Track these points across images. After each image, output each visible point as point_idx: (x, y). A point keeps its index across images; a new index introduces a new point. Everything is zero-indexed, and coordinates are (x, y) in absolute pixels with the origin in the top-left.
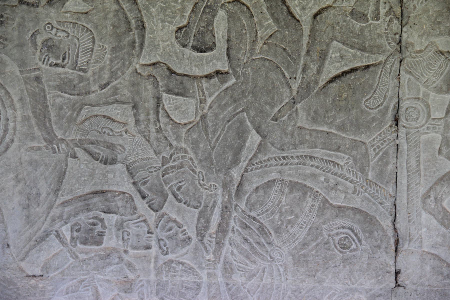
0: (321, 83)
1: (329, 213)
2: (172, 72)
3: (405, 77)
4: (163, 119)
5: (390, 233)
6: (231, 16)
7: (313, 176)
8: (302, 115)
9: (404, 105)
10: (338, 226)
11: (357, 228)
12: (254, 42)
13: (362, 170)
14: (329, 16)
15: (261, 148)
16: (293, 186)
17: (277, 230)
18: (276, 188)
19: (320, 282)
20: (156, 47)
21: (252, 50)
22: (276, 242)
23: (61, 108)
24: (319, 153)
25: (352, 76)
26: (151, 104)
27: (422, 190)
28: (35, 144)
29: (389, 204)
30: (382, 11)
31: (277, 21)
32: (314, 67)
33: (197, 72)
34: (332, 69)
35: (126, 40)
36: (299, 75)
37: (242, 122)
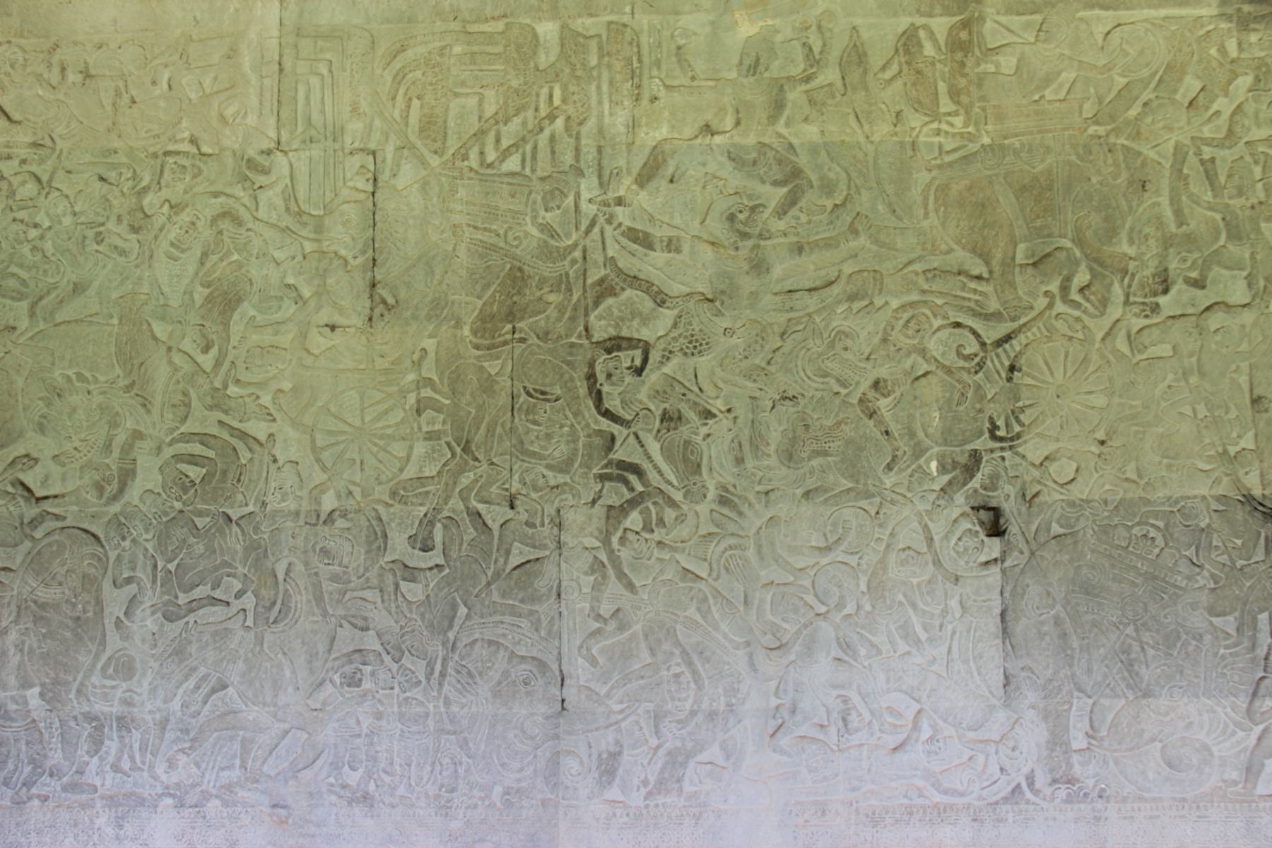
0: (508, 571)
1: (515, 661)
2: (406, 566)
3: (563, 565)
4: (400, 599)
5: (557, 673)
6: (445, 527)
7: (504, 635)
8: (495, 593)
9: (564, 584)
10: (522, 670)
11: (535, 670)
12: (461, 544)
13: (537, 630)
14: (511, 525)
15: (468, 617)
16: (490, 642)
17: (480, 674)
18: (479, 644)
19: (510, 709)
20: (394, 549)
21: (460, 550)
22: (480, 682)
23: (331, 594)
24: (508, 619)
25: (528, 566)
26: (392, 588)
27: (578, 642)
28: (315, 619)
29: (555, 653)
30: (546, 521)
31: (476, 529)
32: (502, 560)
33: (423, 566)
34: (515, 561)
35: (375, 546)
36: (492, 566)
37: (454, 599)
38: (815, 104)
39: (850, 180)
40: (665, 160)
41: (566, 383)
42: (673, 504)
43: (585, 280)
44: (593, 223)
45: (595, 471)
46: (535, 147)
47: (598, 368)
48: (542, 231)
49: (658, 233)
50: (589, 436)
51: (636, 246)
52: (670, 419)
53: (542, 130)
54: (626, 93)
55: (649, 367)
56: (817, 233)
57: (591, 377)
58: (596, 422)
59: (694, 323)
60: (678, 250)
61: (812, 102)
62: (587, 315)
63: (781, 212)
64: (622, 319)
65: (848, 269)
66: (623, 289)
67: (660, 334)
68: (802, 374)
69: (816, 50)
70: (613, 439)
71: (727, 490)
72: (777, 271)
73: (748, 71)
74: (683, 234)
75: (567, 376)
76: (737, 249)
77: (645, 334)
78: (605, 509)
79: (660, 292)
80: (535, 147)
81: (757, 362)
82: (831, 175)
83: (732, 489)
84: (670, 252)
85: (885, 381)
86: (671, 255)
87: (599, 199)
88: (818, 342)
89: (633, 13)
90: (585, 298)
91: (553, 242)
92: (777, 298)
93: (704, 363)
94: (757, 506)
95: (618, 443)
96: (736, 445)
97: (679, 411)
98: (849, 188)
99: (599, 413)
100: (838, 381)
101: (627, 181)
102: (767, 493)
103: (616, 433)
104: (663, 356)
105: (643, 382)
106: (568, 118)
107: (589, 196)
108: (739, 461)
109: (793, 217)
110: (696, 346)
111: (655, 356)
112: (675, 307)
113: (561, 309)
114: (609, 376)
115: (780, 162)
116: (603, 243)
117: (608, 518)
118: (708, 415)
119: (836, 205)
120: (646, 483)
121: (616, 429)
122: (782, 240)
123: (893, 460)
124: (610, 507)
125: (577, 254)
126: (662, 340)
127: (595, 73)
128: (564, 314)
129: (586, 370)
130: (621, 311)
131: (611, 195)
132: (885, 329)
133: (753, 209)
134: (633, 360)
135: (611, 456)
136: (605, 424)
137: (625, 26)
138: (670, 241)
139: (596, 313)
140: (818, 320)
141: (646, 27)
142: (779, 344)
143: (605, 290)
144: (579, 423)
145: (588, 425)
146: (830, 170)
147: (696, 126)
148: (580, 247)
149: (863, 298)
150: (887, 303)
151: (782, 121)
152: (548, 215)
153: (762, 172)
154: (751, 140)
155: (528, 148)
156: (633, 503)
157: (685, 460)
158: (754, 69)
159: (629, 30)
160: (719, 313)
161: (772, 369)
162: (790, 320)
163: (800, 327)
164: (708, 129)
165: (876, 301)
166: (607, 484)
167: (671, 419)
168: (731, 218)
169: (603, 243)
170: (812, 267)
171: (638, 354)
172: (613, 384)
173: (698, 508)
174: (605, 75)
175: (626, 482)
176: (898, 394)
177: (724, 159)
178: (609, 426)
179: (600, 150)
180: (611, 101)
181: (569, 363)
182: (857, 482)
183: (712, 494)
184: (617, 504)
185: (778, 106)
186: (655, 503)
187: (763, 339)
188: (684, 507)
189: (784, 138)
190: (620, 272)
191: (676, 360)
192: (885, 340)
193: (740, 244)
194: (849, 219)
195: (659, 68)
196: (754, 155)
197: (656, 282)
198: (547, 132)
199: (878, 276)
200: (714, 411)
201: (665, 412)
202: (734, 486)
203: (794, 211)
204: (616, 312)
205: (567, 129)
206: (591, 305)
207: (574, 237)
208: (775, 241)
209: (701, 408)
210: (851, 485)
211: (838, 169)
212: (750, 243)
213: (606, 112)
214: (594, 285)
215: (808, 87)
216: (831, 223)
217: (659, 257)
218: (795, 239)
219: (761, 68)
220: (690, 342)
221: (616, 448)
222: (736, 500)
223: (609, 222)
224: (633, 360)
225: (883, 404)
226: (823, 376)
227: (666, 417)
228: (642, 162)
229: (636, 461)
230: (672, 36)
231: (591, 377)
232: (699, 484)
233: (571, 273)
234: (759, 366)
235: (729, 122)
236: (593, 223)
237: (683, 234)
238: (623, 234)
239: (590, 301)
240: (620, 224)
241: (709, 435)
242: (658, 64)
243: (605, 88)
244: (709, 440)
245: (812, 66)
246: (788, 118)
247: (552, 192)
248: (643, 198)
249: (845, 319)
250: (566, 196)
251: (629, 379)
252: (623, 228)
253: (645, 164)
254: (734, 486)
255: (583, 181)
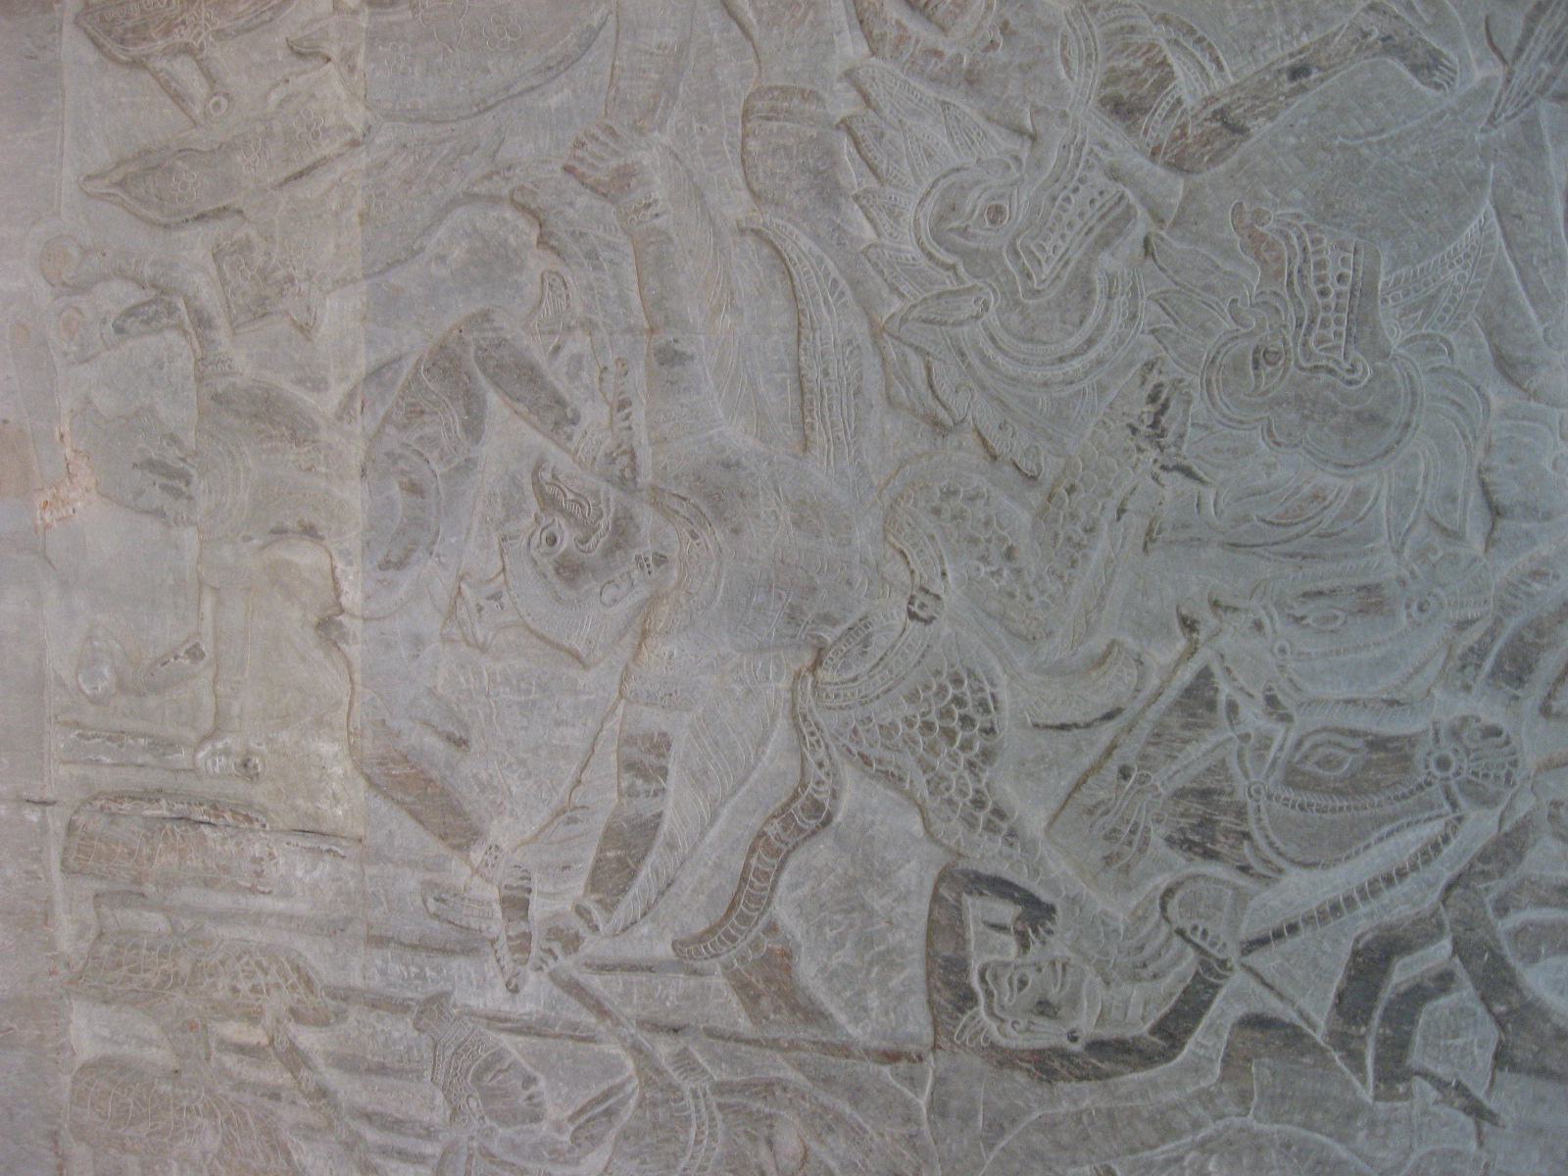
38: (262, 300)
39: (472, 197)
40: (405, 759)
41: (1059, 1146)
42: (1508, 847)
43: (738, 1039)
44: (575, 989)
45: (1367, 1095)
46: (368, 1117)
47: (1016, 1039)
48: (595, 1141)
49: (606, 796)
50: (1244, 1097)
51: (645, 872)
52: (1206, 825)
53: (322, 1092)
54: (230, 846)
55: (1022, 879)
56: (623, 300)
57: (1046, 1065)
58: (1196, 1069)
59: (887, 717)
60: (661, 745)
61: (261, 310)
62: (845, 1050)
63: (558, 416)
64: (866, 941)
65: (737, 207)
66: (772, 928)
67: (917, 827)
68: (1076, 364)
69: (136, 296)
70: (1258, 1023)
71: (1478, 652)
72: (736, 435)
73: (177, 494)
74: (613, 725)
75: (1036, 1139)
76: (661, 560)
77: (916, 874)
78: (1505, 1077)
79: (784, 814)
80: (368, 1117)
81: (1025, 517)
82: (457, 253)
83: (1473, 636)
84: (664, 772)
85: (1112, 78)
86: (673, 769)
87: (507, 961)
88: (969, 308)
89: (44, 803)
90: (794, 1046)
91: (626, 1115)
92: (819, 438)
93: (1017, 695)
94: (1545, 549)
95: (1274, 1007)
96: (1312, 610)
97: (1180, 794)
98: (494, 200)
99: (1166, 1056)
100: (1104, 242)
101: (459, 872)
102: (1496, 512)
103: (1239, 1010)
104: (990, 827)
105: (1073, 901)
106: (295, 1014)
107: (500, 992)
108: (1371, 601)
109: (573, 376)
110: (961, 718)
111: (989, 856)
112: (833, 774)
113: (824, 1122)
114: (1045, 1008)
115: (416, 412)
116: (633, 968)
117: (1543, 1072)
118: (1198, 700)
119: (542, 242)
120: (1426, 931)
121: (1225, 1009)
122: (639, 414)
123: (1402, 51)
124: (1502, 1058)
125: (664, 1048)
126: (939, 826)
127: (187, 924)
128: (839, 1118)
129: (1021, 1078)
130: (839, 943)
131: (496, 925)
132: (934, 80)
133: (549, 502)
134: (1001, 928)
135: (1319, 1037)
136: (1206, 1042)
137: (71, 828)
138: (630, 766)
139: (842, 1018)
140: (897, 305)
141: (77, 770)
142: (970, 439)
143: (771, 981)
144: (1197, 1125)
145: (1206, 1097)
146: (441, 259)
147: (318, 654)
148: (643, 1037)
149: (830, 154)
150: (849, 75)
151: (309, 399)
152: (552, 1112)
153: (440, 469)
154: (353, 495)
155: (372, 1135)
156: (1496, 981)
157: (1352, 787)
158: (173, 478)
159: (81, 819)
160: (860, 634)
161: (1050, 467)
162: (890, 401)
163: (916, 364)
164: (328, 627)
165: (844, 111)
166: (1416, 1058)
167: (1206, 823)
168: (570, 570)
169: (633, 968)
170: (726, 320)
171: (978, 909)
172: (1074, 1001)
173: (1530, 760)
174: (188, 895)
175: (1417, 995)
176: (1159, 34)
177: (406, 580)
178: (1214, 1030)
179: (379, 941)
180: (253, 890)
181: (997, 1127)
182: (1477, 182)
183: (1487, 708)
184: (1491, 1033)
185: (269, 414)
186: (1502, 909)
187: (950, 493)
188: (1524, 806)
189: (351, 396)
190: (716, 934)
191: (1007, 788)
192: (972, 80)
193: (648, 549)
194: (584, 199)
195: (171, 745)
196: (395, 490)
197: (755, 822)
198: (333, 1078)
199: (762, 105)
200: (1186, 675)
201: (1182, 843)
202: (1463, 625)
203: (556, 374)
204: (841, 957)
205: (322, 1022)
206: (813, 1032)
207: (613, 1049)
208: (642, 437)
209: (1175, 721)
210: (1487, 205)
211: (441, 233)
212: (647, 518)
213: (281, 905)
214: (755, 1017)
215: (221, 321)
216: (592, 255)
217: (678, 806)
218: (639, 374)
219: (172, 455)
220: (949, 735)
221: (1290, 1015)
222: (1512, 624)
223: (572, 943)
224: (1001, 928)
225: (1191, 85)
226: (1087, 296)
227: (1198, 842)
228: (410, 824)
229: (1345, 956)
230: (94, 700)
231: (1046, 1065)
232: (1447, 749)
233: (721, 1074)
234: (1041, 514)
235: (305, 557)
236: (575, 989)
237: (613, 725)
238: (609, 907)
239: (806, 1033)
240: (581, 911)
241: (1271, 701)
242: (163, 746)
243: (221, 900)
244: (1288, 703)
245: (171, 310)
246: (300, 382)
247: (488, 1096)
248: (503, 832)
249: (894, 214)
250: (499, 1056)
251: (1059, 944)
252: (589, 903)
253: (415, 815)
254: (1463, 625)
255: (457, 996)
